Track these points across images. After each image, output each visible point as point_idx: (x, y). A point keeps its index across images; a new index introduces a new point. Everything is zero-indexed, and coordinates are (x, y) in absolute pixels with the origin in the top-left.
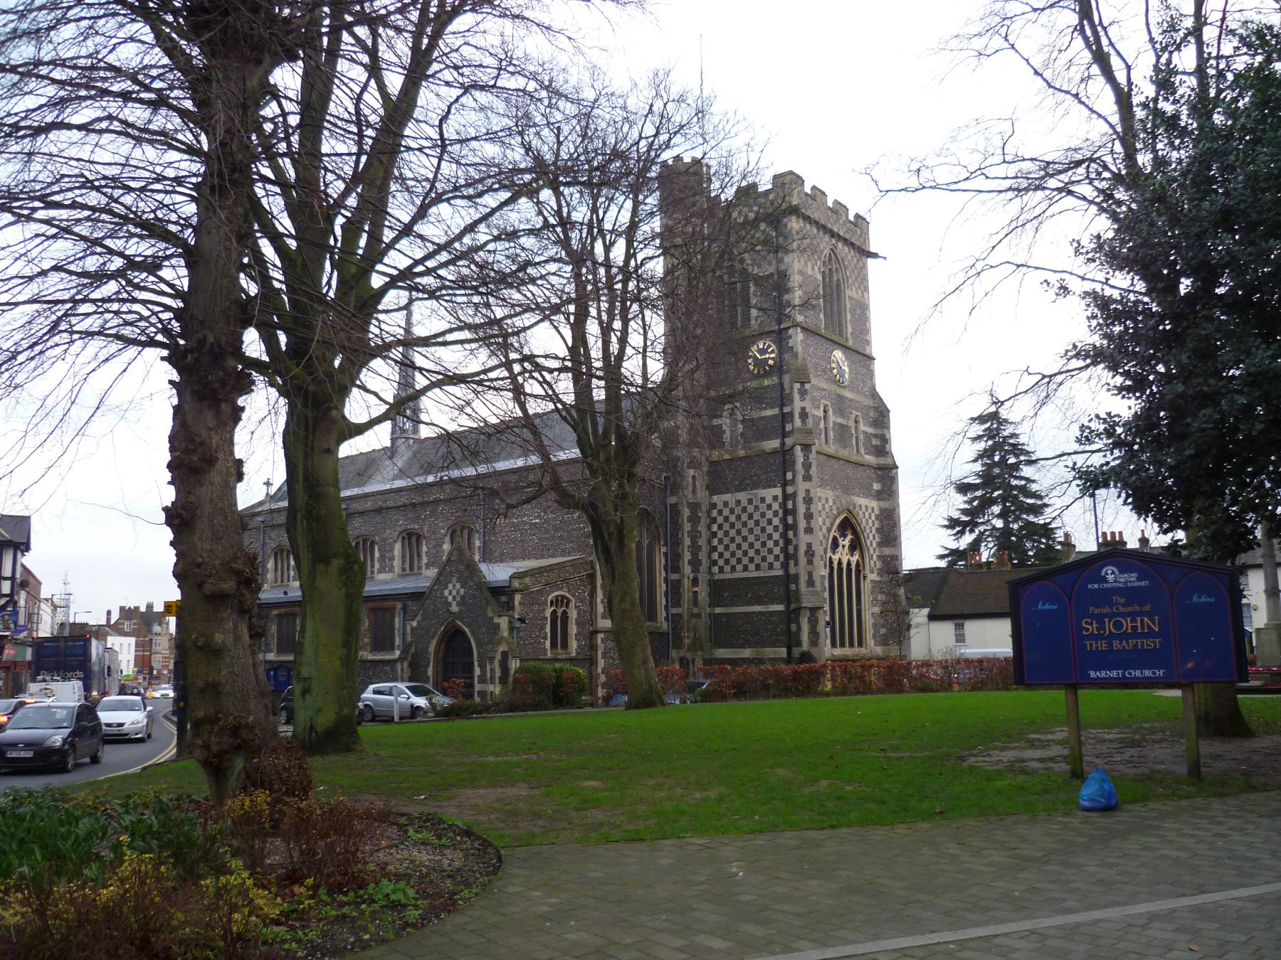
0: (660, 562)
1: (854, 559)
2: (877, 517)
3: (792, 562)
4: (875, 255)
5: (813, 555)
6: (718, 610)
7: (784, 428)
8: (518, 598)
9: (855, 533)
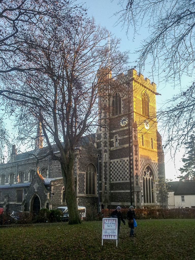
0: (96, 178)
1: (151, 178)
2: (158, 166)
3: (132, 178)
4: (157, 94)
5: (138, 176)
6: (112, 192)
7: (130, 141)
8: (52, 187)
9: (151, 170)
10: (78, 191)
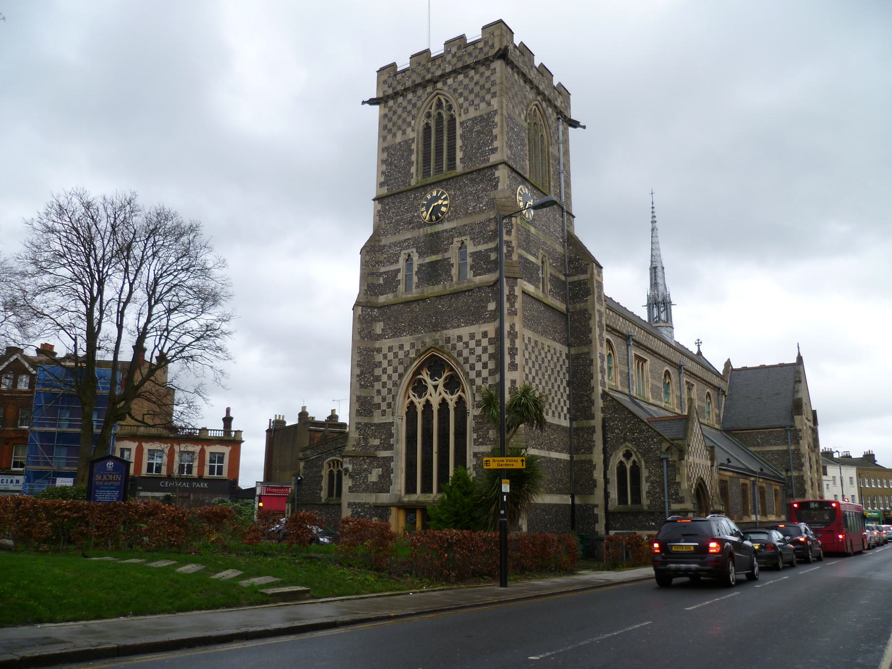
1: (452, 400)
9: (452, 369)
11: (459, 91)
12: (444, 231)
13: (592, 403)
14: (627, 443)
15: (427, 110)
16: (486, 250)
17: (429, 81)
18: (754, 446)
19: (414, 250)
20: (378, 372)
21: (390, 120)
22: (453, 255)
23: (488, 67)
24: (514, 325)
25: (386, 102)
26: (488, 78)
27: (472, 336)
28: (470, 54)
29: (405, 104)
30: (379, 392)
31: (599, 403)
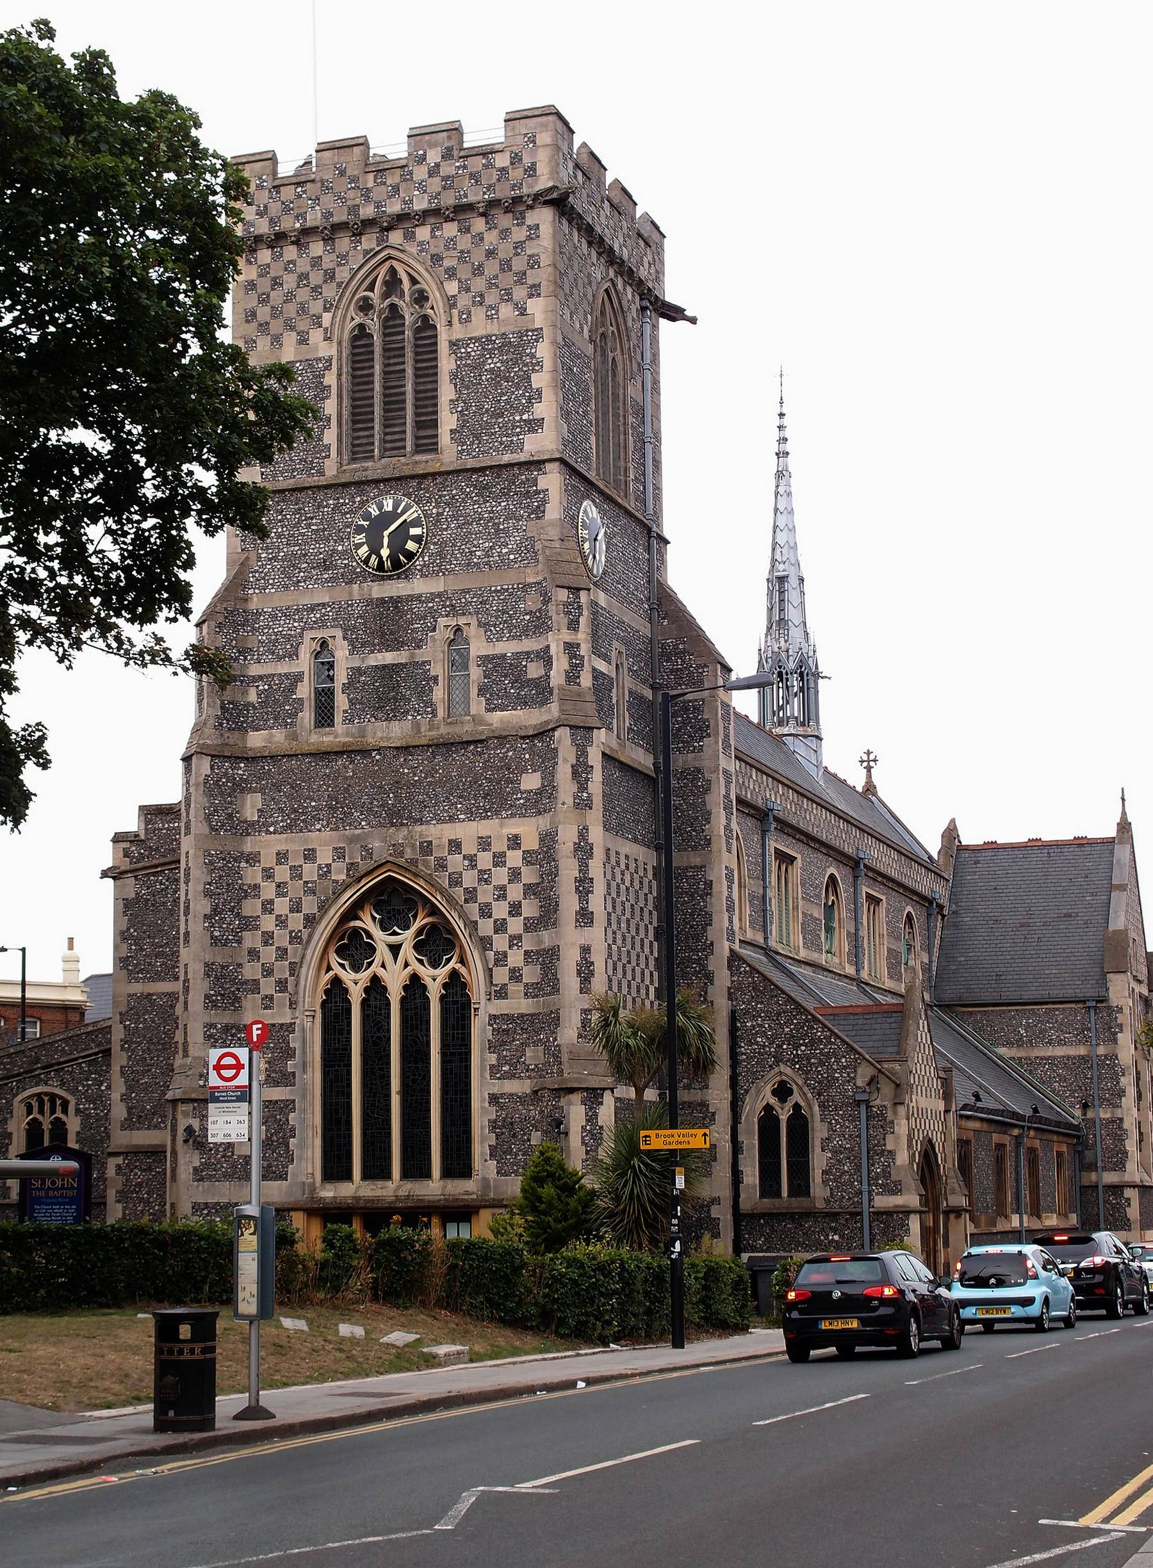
1: (434, 979)
9: (434, 911)
10: (119, 1111)
11: (447, 263)
12: (411, 598)
13: (709, 977)
14: (782, 1067)
15: (362, 294)
16: (517, 655)
17: (368, 223)
18: (1009, 1044)
19: (339, 633)
20: (251, 907)
21: (264, 300)
22: (433, 654)
23: (521, 219)
24: (586, 828)
25: (253, 251)
26: (519, 245)
27: (484, 843)
28: (475, 177)
29: (303, 265)
30: (254, 954)
31: (723, 978)
